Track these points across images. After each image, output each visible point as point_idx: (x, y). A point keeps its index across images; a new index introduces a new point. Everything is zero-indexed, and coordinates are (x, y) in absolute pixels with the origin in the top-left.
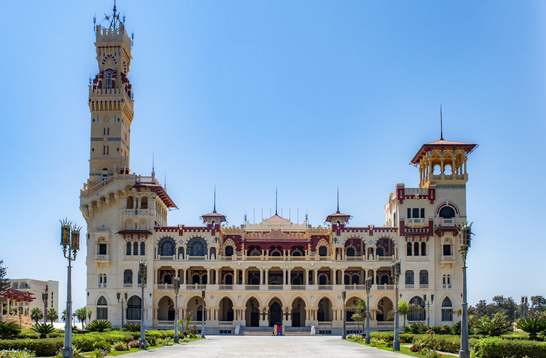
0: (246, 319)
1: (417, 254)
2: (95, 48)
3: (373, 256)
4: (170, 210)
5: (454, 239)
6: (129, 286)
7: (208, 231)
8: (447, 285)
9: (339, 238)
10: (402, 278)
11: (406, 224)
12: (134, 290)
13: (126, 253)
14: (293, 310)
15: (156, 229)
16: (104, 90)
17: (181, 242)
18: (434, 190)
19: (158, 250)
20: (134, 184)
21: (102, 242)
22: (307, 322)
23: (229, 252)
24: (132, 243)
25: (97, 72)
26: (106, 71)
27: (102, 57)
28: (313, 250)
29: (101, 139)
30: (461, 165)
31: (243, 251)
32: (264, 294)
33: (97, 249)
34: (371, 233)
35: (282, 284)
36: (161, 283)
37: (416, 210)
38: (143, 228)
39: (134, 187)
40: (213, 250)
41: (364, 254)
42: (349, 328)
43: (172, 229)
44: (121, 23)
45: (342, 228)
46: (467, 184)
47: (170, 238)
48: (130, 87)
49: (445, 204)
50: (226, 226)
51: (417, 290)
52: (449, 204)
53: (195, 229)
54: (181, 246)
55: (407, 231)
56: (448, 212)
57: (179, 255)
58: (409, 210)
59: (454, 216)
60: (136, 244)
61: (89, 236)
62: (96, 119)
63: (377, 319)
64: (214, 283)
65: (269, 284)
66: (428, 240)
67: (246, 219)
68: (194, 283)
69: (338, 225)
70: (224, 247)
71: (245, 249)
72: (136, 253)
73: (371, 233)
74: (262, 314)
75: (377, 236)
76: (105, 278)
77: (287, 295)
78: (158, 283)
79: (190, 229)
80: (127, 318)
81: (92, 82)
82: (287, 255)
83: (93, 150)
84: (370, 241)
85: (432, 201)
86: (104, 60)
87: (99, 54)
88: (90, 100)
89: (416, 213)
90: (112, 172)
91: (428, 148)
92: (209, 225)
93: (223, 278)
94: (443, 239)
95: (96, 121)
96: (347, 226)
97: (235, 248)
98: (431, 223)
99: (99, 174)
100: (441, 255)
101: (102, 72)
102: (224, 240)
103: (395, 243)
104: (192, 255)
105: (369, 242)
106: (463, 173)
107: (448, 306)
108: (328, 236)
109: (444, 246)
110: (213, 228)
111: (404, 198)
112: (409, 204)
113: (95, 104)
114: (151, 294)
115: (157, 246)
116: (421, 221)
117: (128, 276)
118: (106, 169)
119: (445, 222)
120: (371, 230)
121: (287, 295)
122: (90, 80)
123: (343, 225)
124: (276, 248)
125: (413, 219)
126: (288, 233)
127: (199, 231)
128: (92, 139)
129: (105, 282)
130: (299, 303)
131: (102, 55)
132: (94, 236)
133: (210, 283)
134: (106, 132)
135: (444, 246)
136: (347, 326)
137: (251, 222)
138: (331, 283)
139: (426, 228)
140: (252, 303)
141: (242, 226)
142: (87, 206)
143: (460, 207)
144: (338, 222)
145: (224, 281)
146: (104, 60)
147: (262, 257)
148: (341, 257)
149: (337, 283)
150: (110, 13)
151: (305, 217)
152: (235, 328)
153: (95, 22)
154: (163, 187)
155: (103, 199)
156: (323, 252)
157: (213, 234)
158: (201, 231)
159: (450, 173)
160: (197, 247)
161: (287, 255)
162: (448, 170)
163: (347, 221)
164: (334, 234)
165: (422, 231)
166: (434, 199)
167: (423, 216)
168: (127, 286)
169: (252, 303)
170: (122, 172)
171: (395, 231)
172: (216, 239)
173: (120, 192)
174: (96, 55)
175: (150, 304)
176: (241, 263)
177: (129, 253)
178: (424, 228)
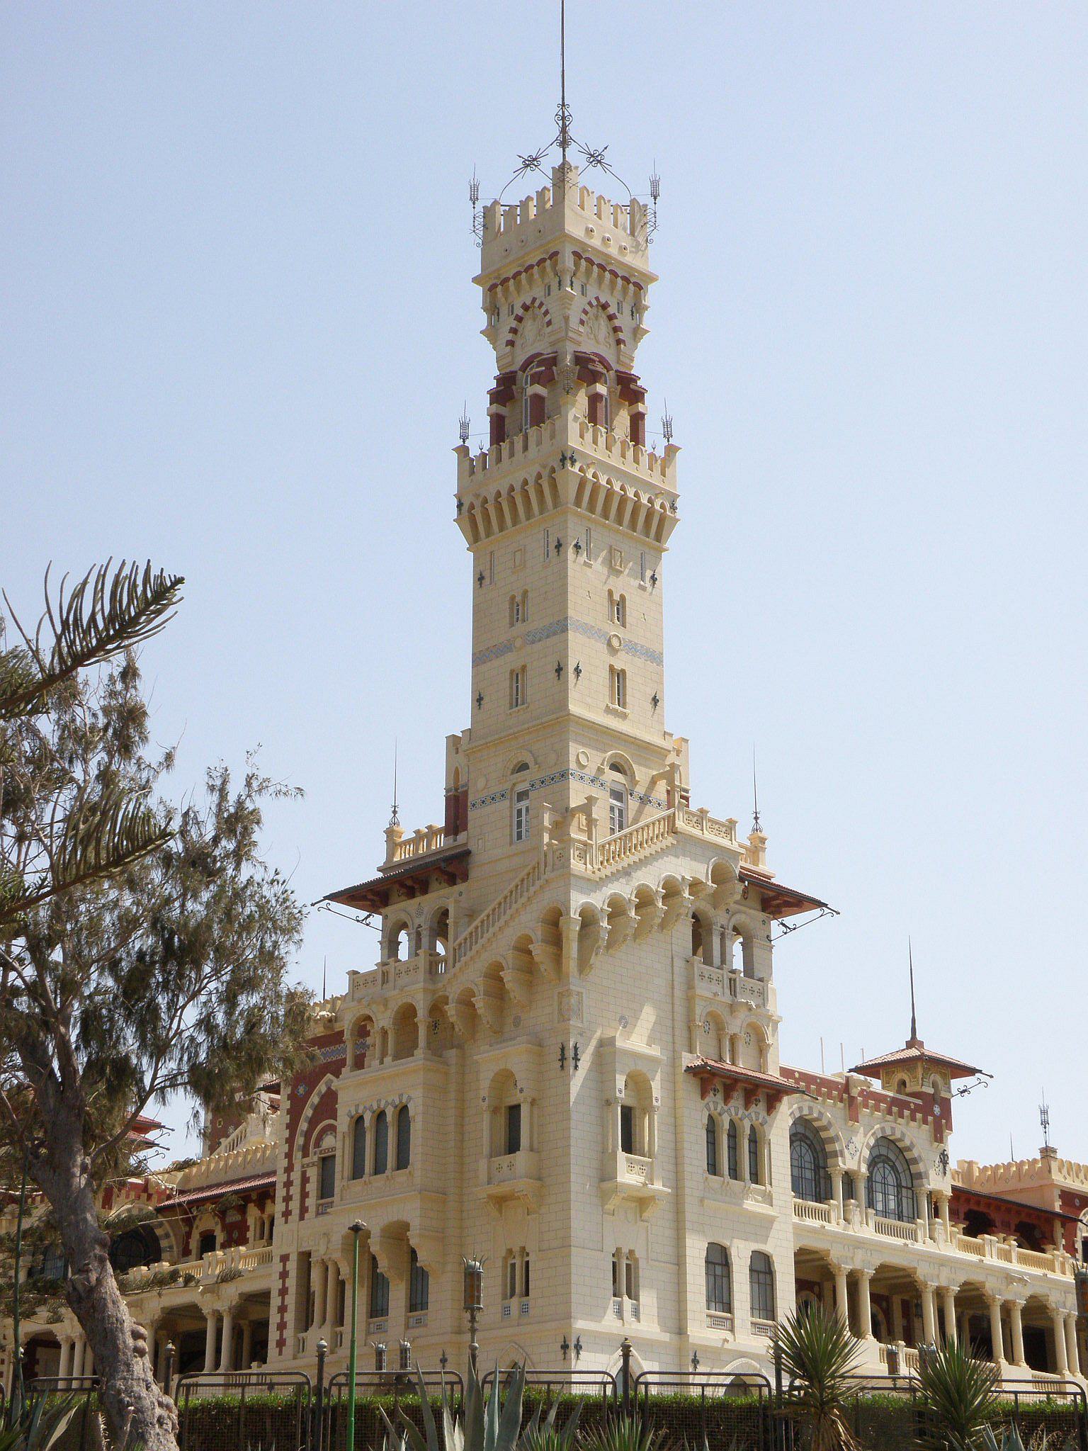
2: (477, 294)
26: (524, 367)
62: (487, 574)
87: (492, 308)
95: (487, 581)
113: (477, 512)
131: (504, 310)
153: (474, 200)
174: (482, 320)
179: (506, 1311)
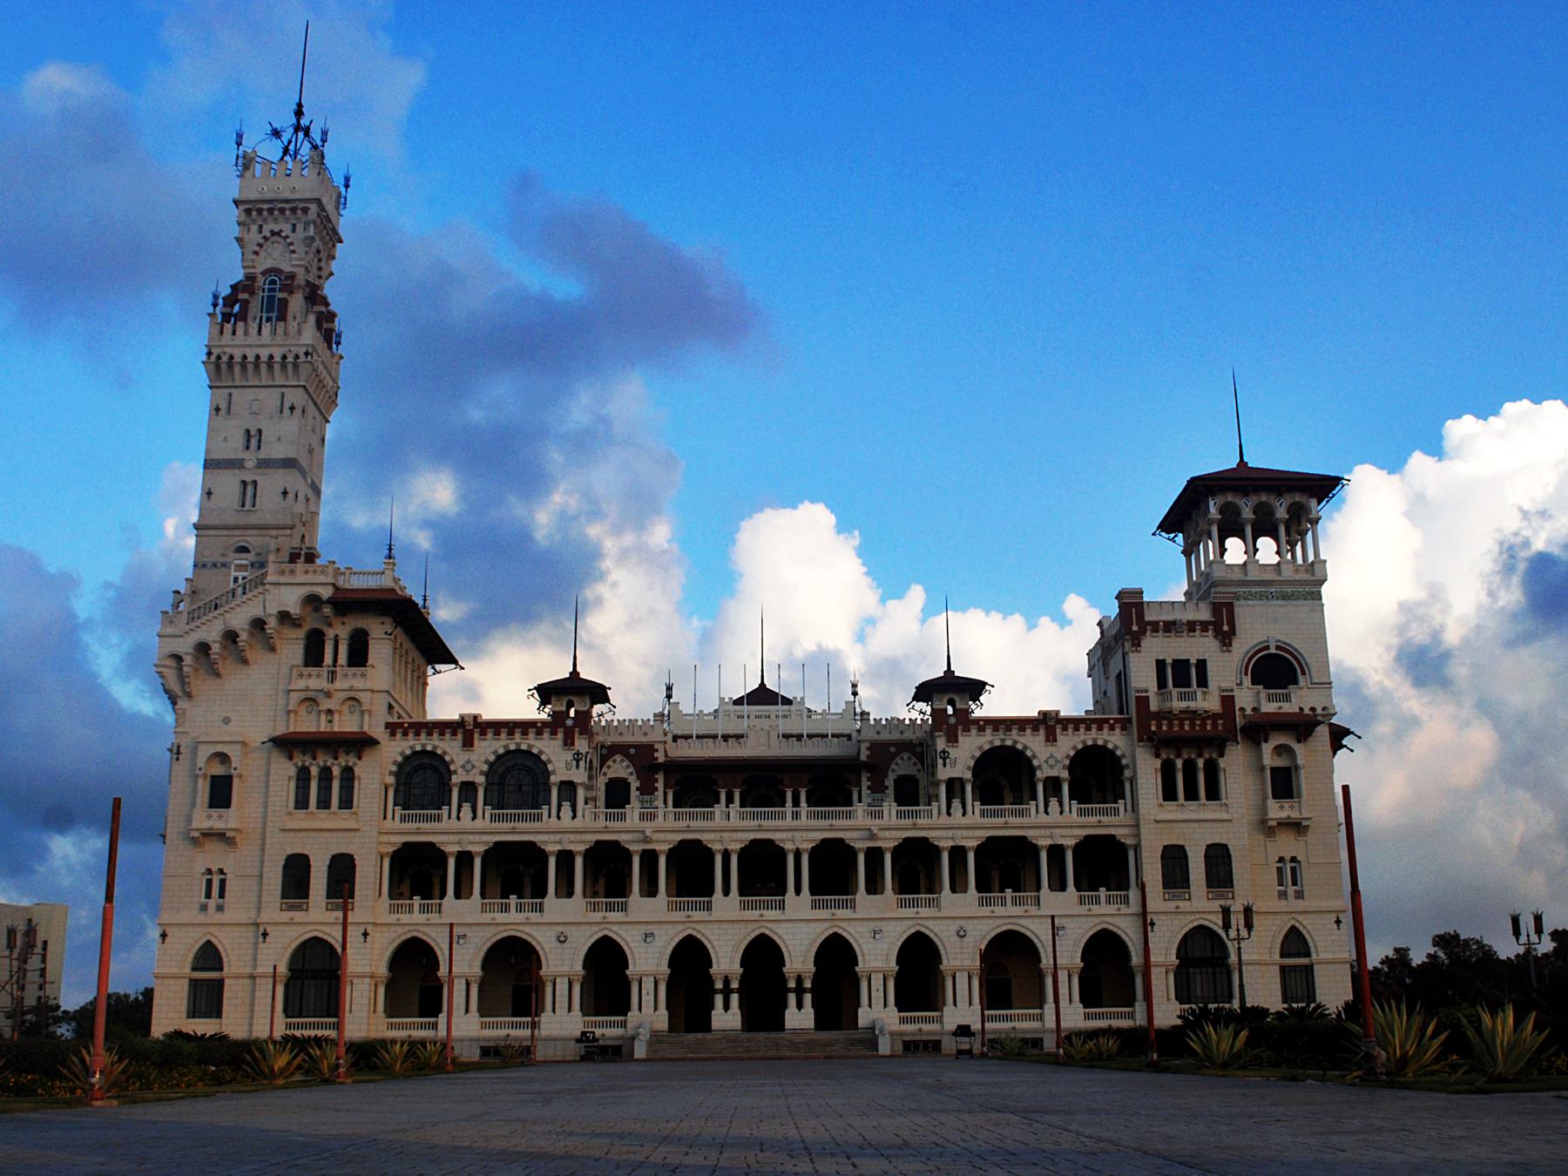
0: (668, 1008)
1: (1191, 795)
3: (1061, 805)
4: (436, 672)
5: (1299, 749)
6: (298, 908)
7: (554, 733)
8: (1291, 890)
9: (953, 753)
10: (1153, 872)
11: (1154, 706)
12: (318, 918)
13: (292, 803)
14: (816, 979)
15: (392, 728)
16: (253, 327)
17: (468, 766)
18: (1230, 607)
19: (396, 791)
20: (326, 593)
21: (219, 770)
22: (864, 1016)
23: (617, 795)
24: (314, 771)
25: (239, 275)
26: (263, 273)
27: (254, 236)
28: (878, 788)
29: (236, 464)
30: (1303, 534)
31: (660, 793)
32: (726, 928)
33: (203, 788)
34: (1051, 738)
35: (783, 892)
36: (400, 896)
37: (1181, 666)
38: (346, 724)
39: (330, 601)
40: (568, 789)
41: (1035, 798)
42: (994, 1031)
43: (443, 727)
44: (315, 147)
45: (966, 721)
46: (1325, 589)
47: (433, 754)
48: (332, 316)
49: (1267, 648)
50: (608, 717)
51: (1201, 906)
52: (1278, 648)
53: (511, 727)
54: (469, 778)
55: (1159, 726)
56: (1277, 669)
57: (460, 807)
58: (1161, 664)
59: (1296, 682)
60: (326, 773)
61: (178, 753)
63: (1081, 1001)
64: (570, 894)
65: (742, 893)
66: (1222, 755)
67: (669, 697)
68: (505, 896)
69: (950, 710)
70: (601, 782)
71: (666, 786)
72: (324, 803)
73: (1051, 738)
74: (721, 991)
75: (1068, 744)
76: (223, 883)
77: (799, 928)
78: (391, 897)
79: (498, 727)
80: (287, 1012)
81: (221, 301)
82: (796, 803)
83: (209, 493)
84: (1052, 759)
85: (1226, 638)
86: (260, 245)
88: (209, 354)
89: (1183, 673)
90: (261, 559)
91: (1198, 491)
92: (554, 715)
93: (596, 881)
94: (1267, 748)
96: (978, 713)
97: (634, 783)
98: (1228, 701)
99: (224, 565)
100: (1265, 799)
101: (250, 278)
102: (604, 760)
103: (1124, 762)
104: (500, 805)
105: (1046, 761)
106: (1311, 558)
107: (1298, 955)
108: (921, 744)
109: (1272, 769)
110: (569, 723)
111: (1142, 632)
112: (1156, 647)
114: (371, 935)
115: (391, 780)
116: (1199, 694)
117: (296, 873)
118: (243, 550)
119: (1270, 699)
120: (1048, 723)
121: (799, 928)
122: (216, 297)
123: (968, 712)
124: (762, 782)
125: (1175, 692)
126: (799, 737)
127: (525, 733)
128: (210, 464)
129: (222, 895)
130: (836, 956)
132: (195, 752)
133: (557, 895)
134: (254, 442)
135: (1272, 769)
136: (988, 1026)
137: (686, 708)
138: (933, 887)
139: (1214, 717)
140: (690, 958)
141: (660, 717)
142: (178, 658)
143: (1310, 658)
144: (951, 702)
145: (601, 887)
146: (260, 245)
147: (719, 809)
148: (964, 807)
149: (953, 890)
150: (286, 121)
151: (850, 690)
152: (633, 1038)
153: (239, 144)
154: (420, 602)
155: (231, 637)
156: (908, 794)
157: (568, 742)
158: (532, 731)
159: (1275, 559)
160: (518, 778)
161: (796, 803)
162: (1267, 550)
163: (975, 698)
164: (941, 744)
165: (1204, 725)
166: (1232, 631)
167: (1203, 682)
168: (291, 908)
169: (690, 958)
170: (294, 558)
171: (1123, 729)
172: (578, 757)
173: (284, 617)
175: (366, 963)
176: (655, 825)
177: (302, 803)
178: (1208, 718)
179: (204, 908)
